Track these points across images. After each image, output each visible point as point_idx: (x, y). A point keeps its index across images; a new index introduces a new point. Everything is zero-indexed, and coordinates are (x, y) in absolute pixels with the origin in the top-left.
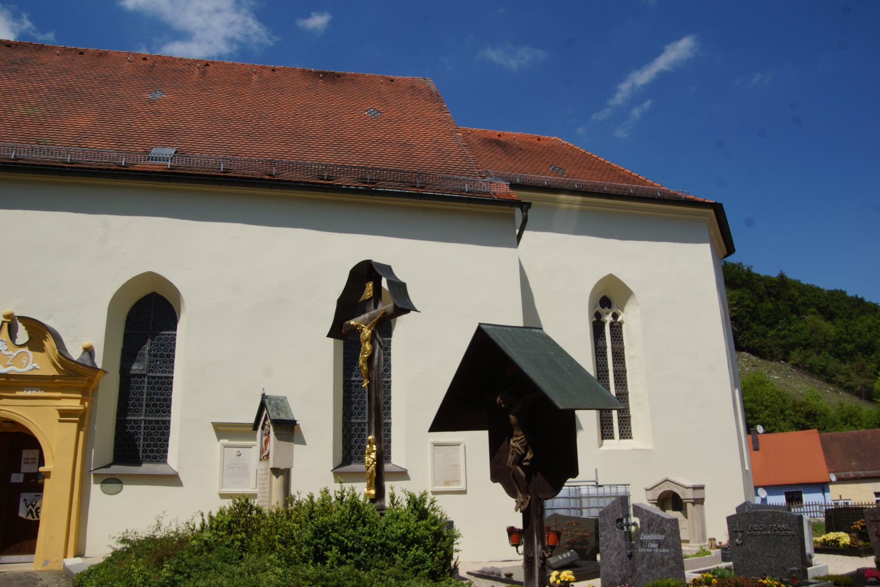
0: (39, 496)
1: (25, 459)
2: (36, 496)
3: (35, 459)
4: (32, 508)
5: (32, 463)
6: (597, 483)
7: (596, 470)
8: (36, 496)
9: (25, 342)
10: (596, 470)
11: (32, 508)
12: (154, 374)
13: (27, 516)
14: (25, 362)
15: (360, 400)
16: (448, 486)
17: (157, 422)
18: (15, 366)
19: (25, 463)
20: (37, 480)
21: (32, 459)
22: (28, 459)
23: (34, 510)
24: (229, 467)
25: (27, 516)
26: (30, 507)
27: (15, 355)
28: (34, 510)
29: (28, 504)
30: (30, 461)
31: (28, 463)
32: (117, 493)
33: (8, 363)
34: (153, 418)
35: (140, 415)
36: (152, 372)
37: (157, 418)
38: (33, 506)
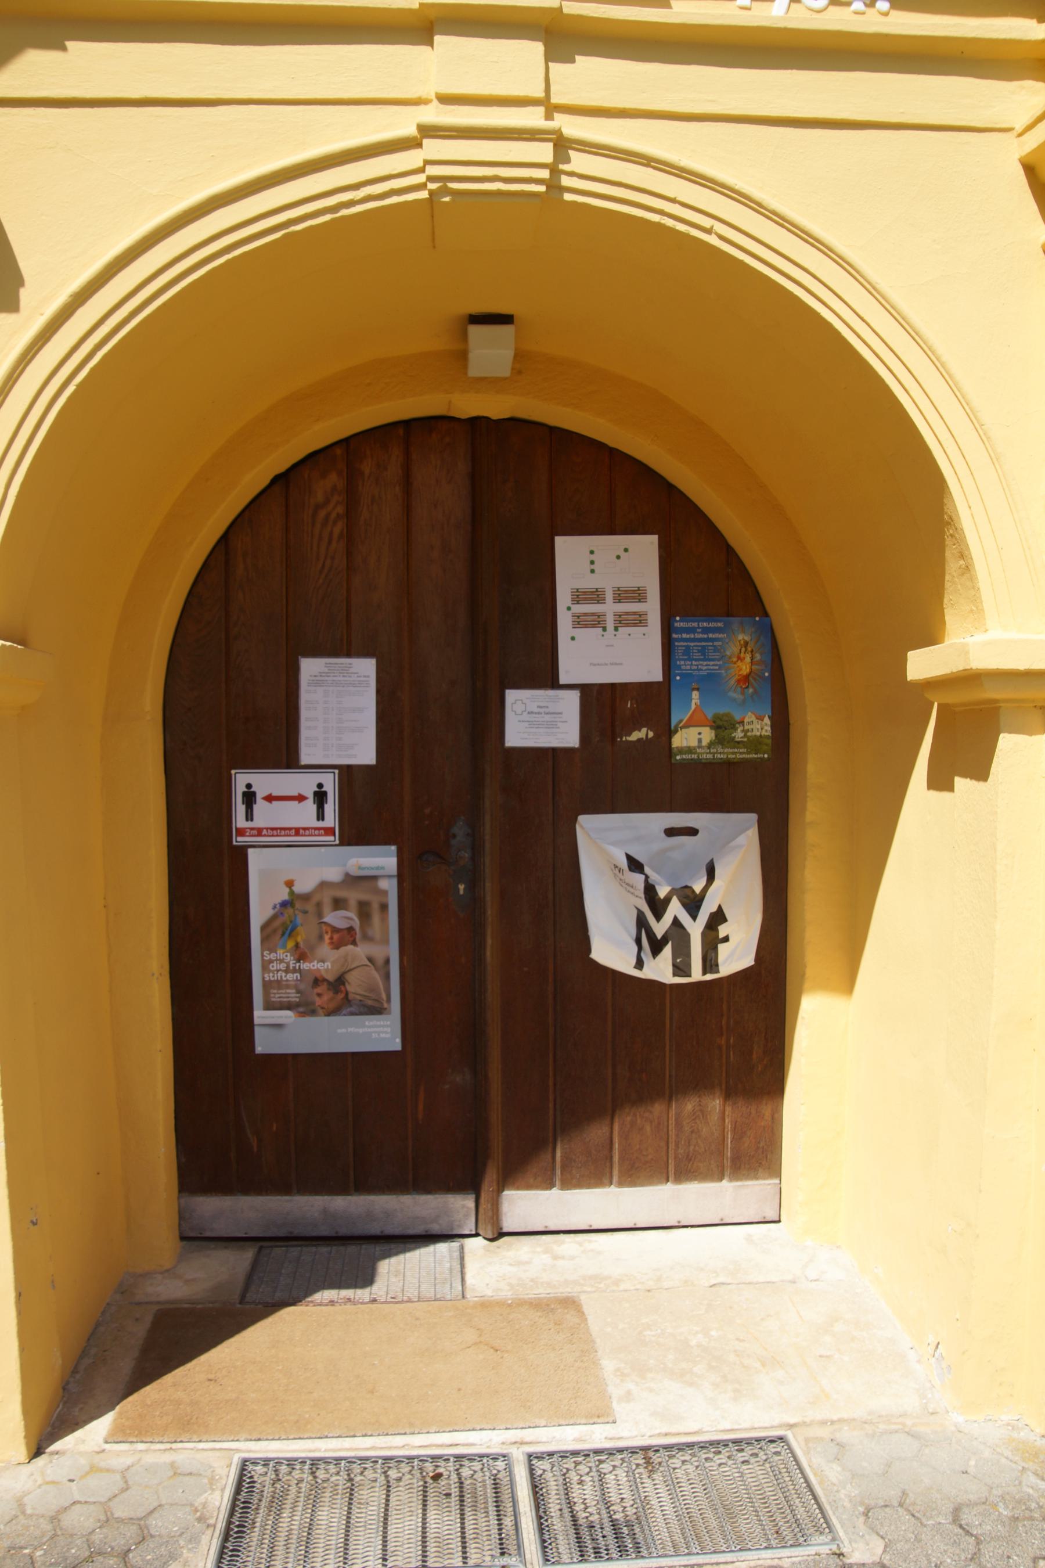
0: (692, 832)
1: (579, 596)
2: (671, 832)
3: (638, 595)
4: (685, 918)
5: (623, 621)
8: (671, 832)
11: (685, 918)
13: (639, 964)
19: (580, 622)
20: (670, 733)
21: (621, 595)
22: (596, 596)
23: (695, 929)
25: (639, 964)
26: (675, 909)
28: (695, 929)
29: (662, 892)
30: (610, 608)
31: (596, 621)
38: (693, 904)
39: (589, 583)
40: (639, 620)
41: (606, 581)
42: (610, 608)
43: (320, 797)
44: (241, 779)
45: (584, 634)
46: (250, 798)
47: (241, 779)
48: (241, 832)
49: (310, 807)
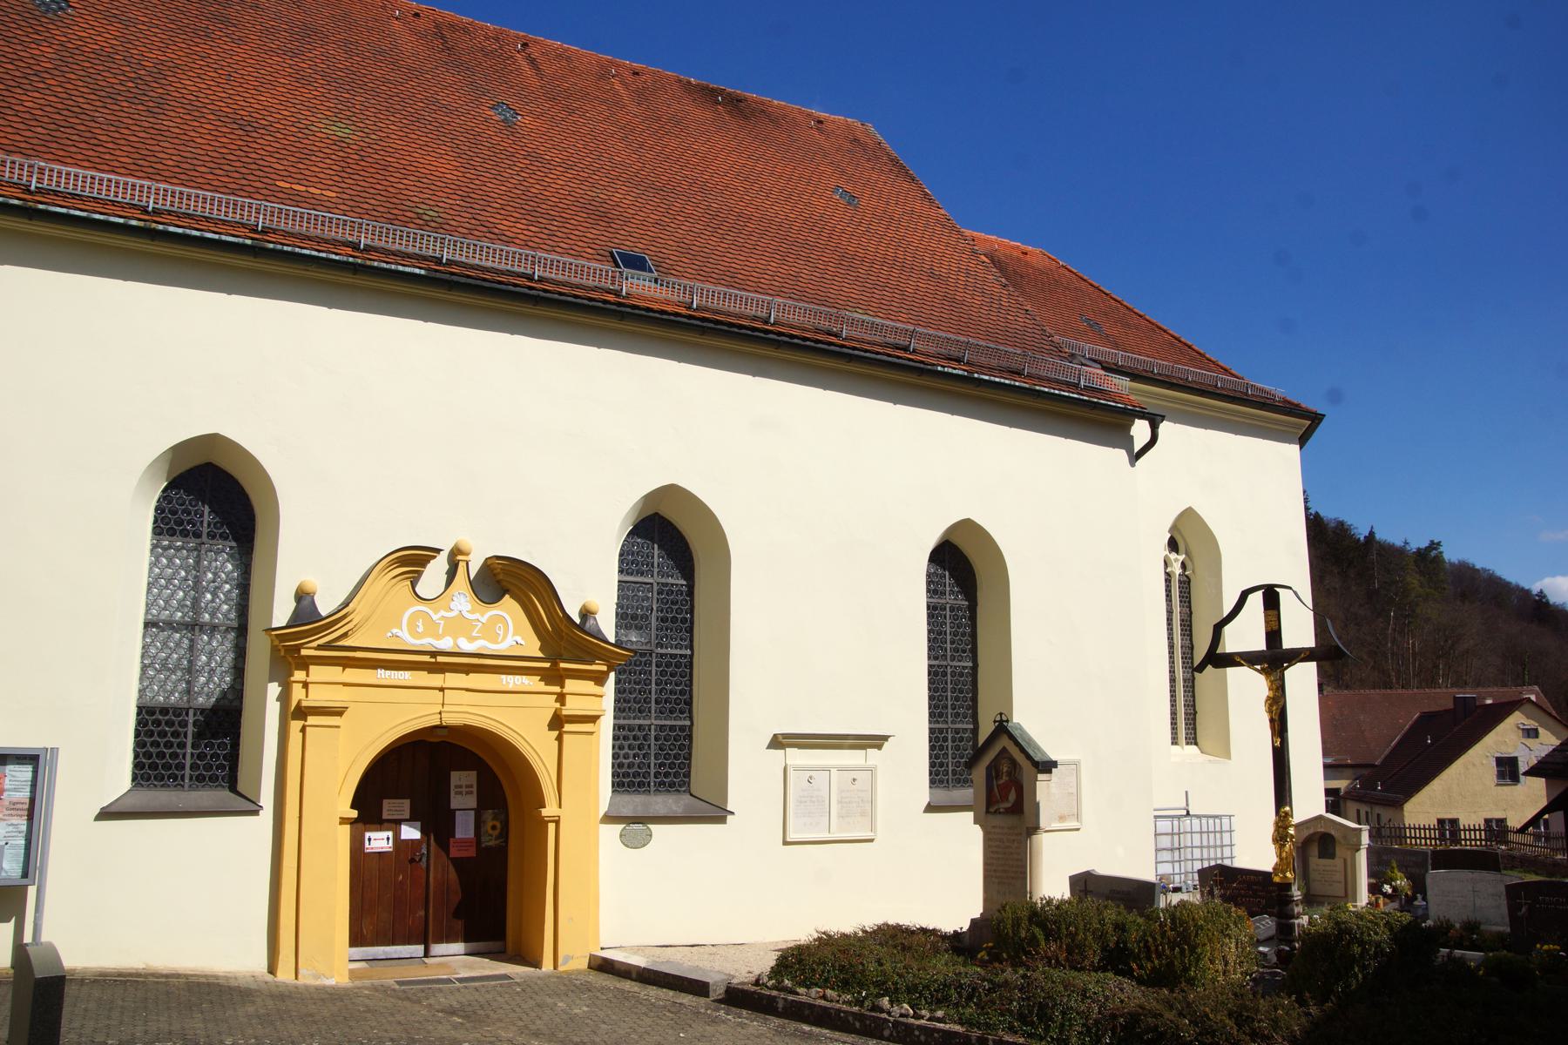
1: (456, 787)
5: (467, 793)
6: (1188, 812)
7: (1186, 792)
9: (567, 611)
10: (1186, 792)
12: (663, 651)
14: (501, 633)
15: (941, 695)
16: (1063, 822)
17: (672, 728)
18: (484, 639)
19: (456, 793)
21: (467, 786)
22: (461, 787)
24: (801, 802)
27: (484, 620)
30: (464, 790)
31: (461, 793)
32: (644, 845)
33: (474, 634)
34: (668, 723)
35: (646, 718)
36: (662, 648)
37: (673, 723)
39: (459, 783)
40: (471, 793)
41: (464, 782)
42: (464, 790)
43: (388, 839)
44: (367, 835)
45: (459, 797)
46: (370, 840)
47: (367, 835)
48: (367, 849)
49: (385, 841)
